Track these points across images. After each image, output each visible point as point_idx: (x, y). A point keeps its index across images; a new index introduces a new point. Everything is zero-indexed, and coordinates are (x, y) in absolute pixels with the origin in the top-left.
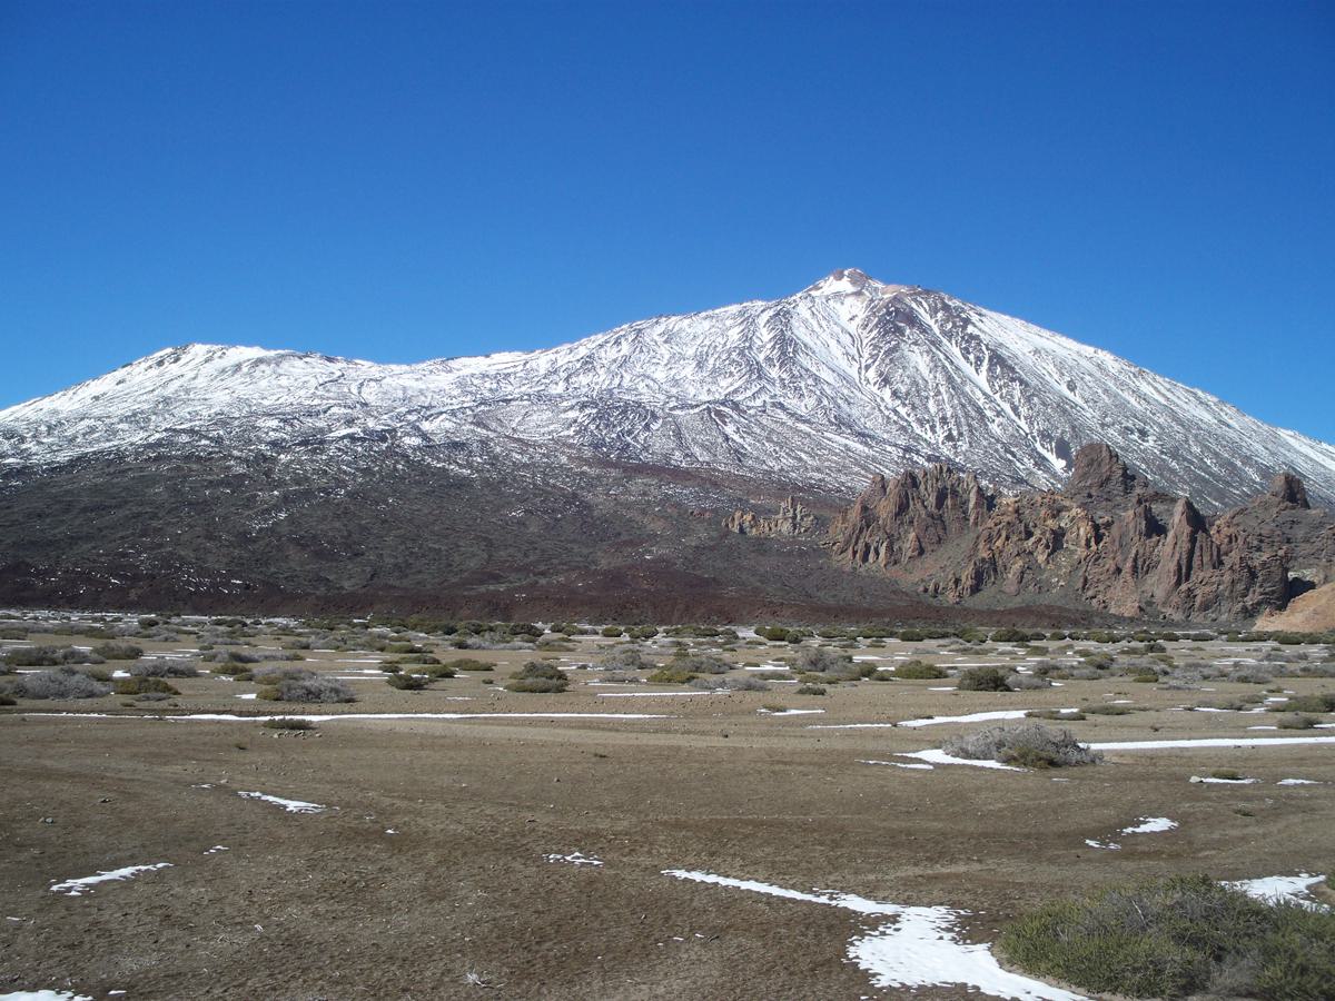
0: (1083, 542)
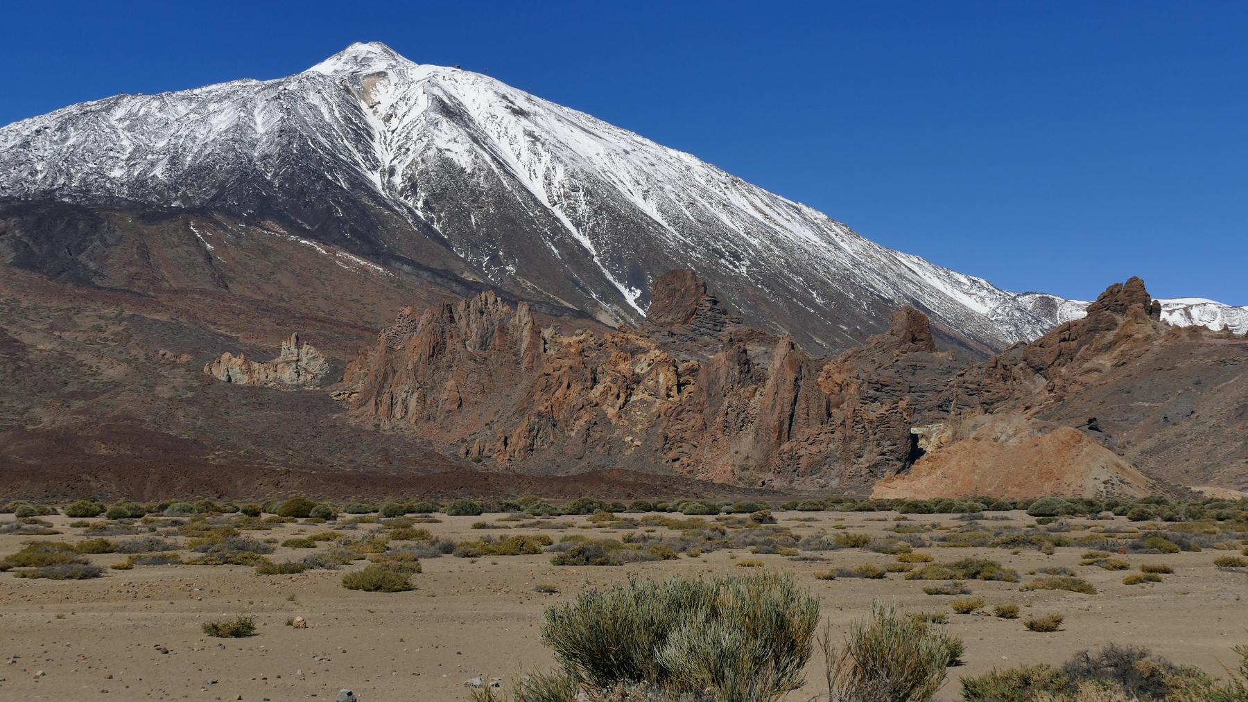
0: (663, 392)
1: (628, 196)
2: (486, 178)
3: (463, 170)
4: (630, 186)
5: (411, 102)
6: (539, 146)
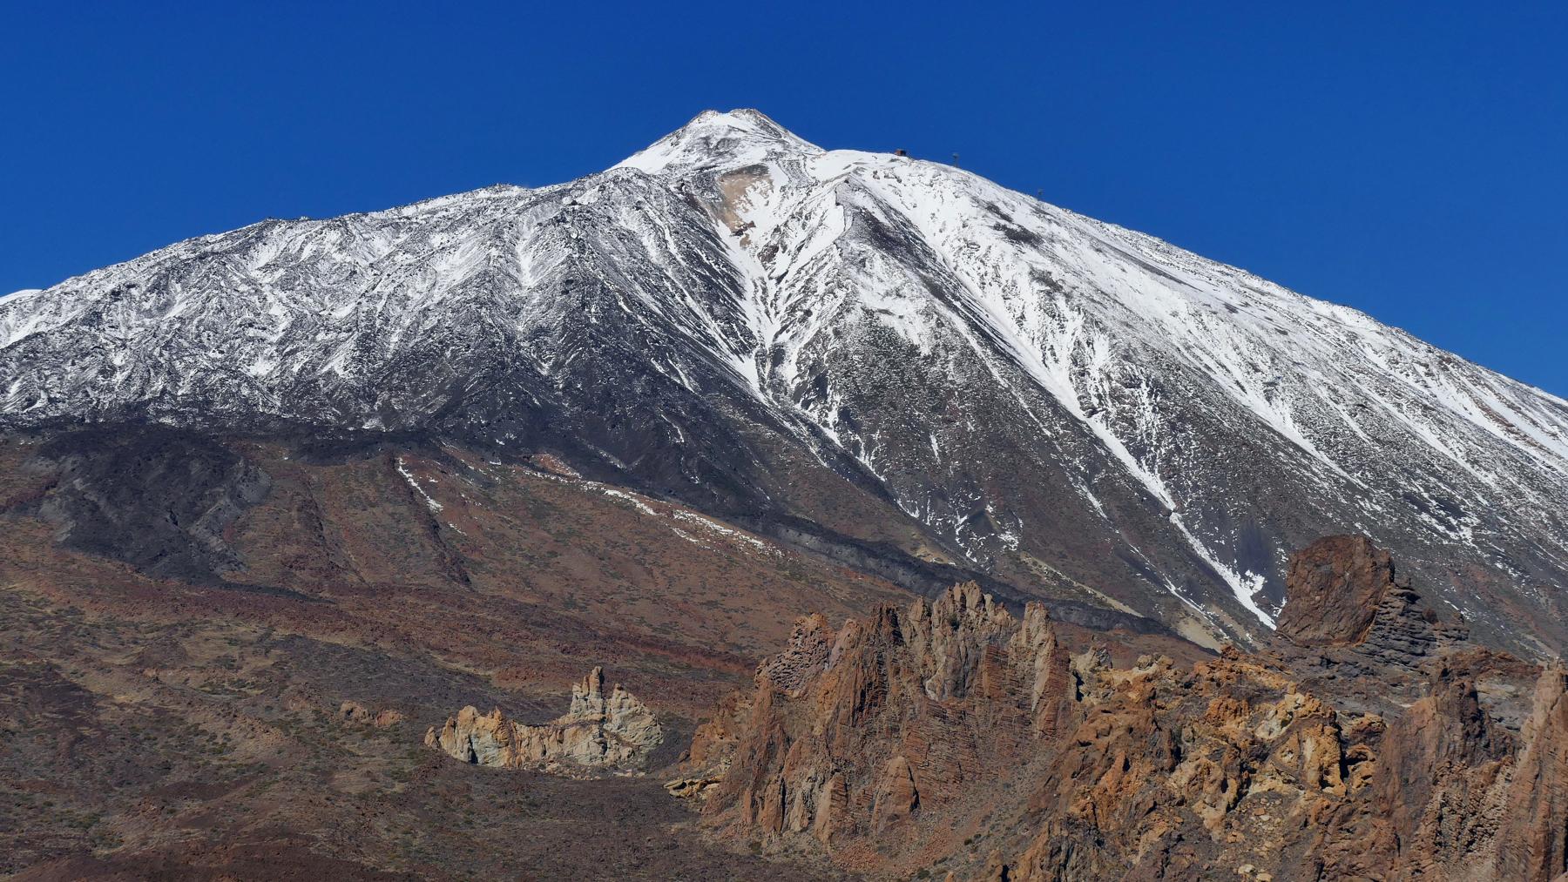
0: (1312, 776)
1: (1236, 393)
2: (958, 364)
3: (913, 350)
4: (1238, 374)
5: (814, 222)
6: (1061, 301)
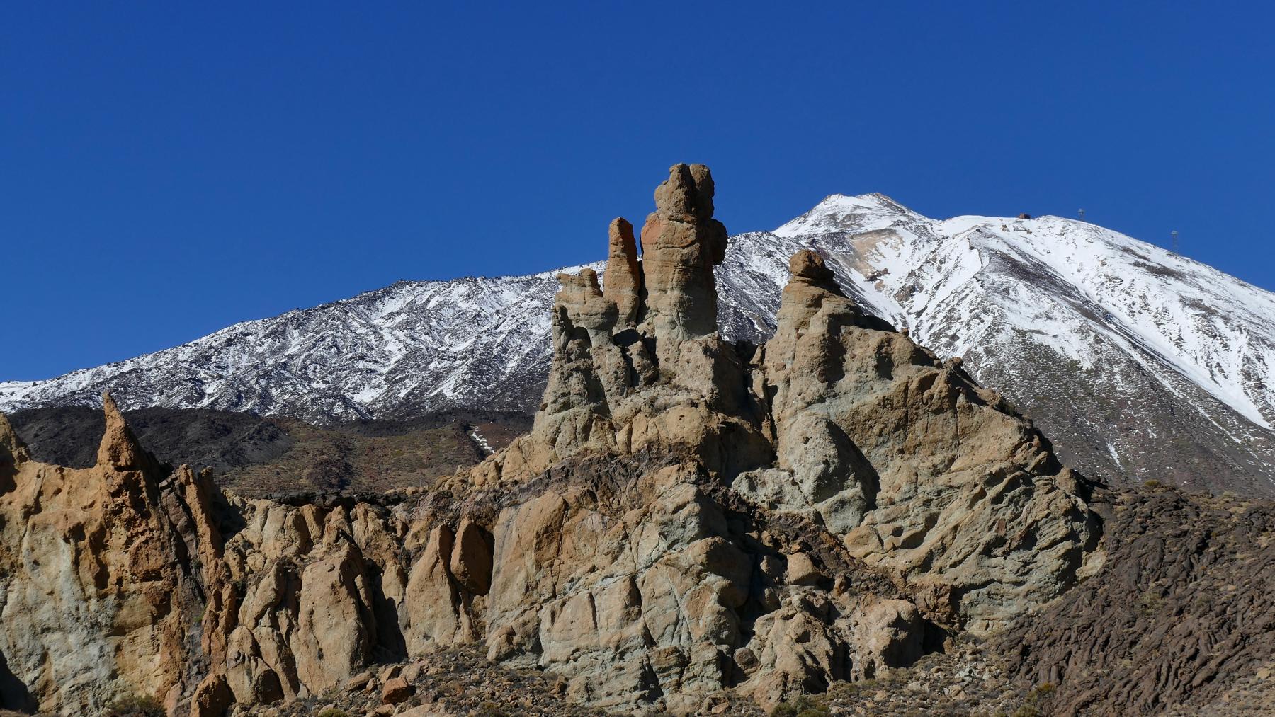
2: (1126, 376)
3: (1074, 366)
5: (949, 265)
6: (1219, 323)
